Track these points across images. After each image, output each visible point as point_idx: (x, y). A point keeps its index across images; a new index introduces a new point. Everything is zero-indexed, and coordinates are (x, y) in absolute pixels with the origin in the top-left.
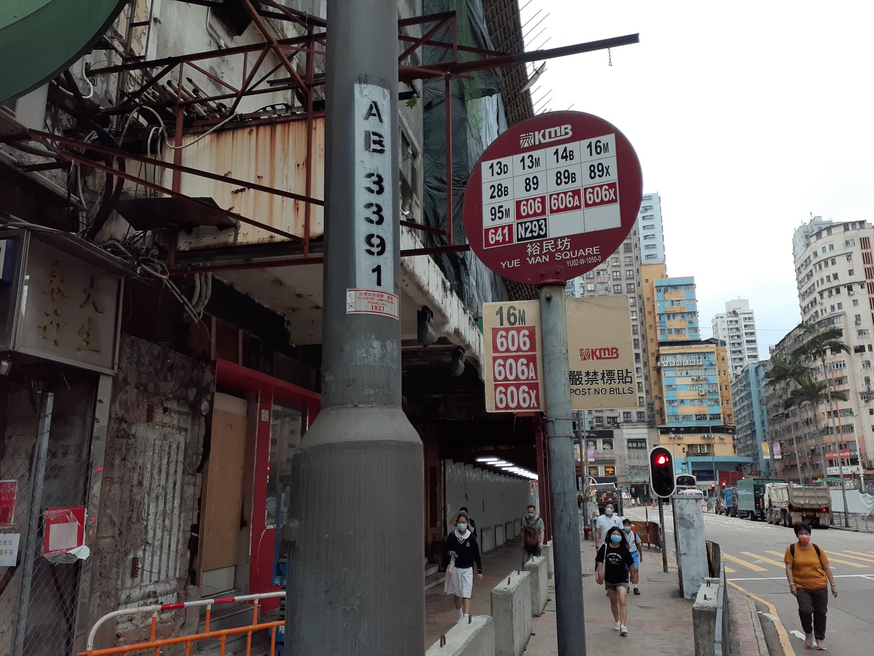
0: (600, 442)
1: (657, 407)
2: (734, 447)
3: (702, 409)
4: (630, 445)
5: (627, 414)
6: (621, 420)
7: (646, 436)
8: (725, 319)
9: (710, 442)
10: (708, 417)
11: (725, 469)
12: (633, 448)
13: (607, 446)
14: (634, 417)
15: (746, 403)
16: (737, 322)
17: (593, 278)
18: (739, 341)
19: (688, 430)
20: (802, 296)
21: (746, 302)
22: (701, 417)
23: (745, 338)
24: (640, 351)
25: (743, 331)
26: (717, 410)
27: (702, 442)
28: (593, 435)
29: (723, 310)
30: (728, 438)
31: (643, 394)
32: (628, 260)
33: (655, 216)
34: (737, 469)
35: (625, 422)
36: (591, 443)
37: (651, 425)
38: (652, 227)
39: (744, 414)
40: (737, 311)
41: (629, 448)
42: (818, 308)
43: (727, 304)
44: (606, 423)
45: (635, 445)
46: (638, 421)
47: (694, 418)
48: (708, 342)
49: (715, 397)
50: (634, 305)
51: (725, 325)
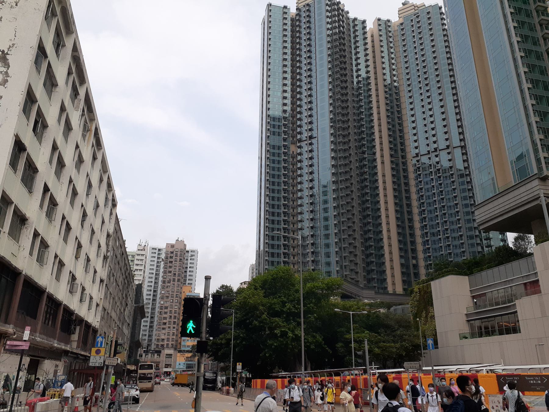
0: (156, 355)
1: (179, 341)
5: (168, 344)
6: (165, 346)
14: (170, 346)
19: (188, 351)
24: (176, 320)
31: (175, 337)
37: (175, 349)
44: (160, 347)
50: (177, 303)
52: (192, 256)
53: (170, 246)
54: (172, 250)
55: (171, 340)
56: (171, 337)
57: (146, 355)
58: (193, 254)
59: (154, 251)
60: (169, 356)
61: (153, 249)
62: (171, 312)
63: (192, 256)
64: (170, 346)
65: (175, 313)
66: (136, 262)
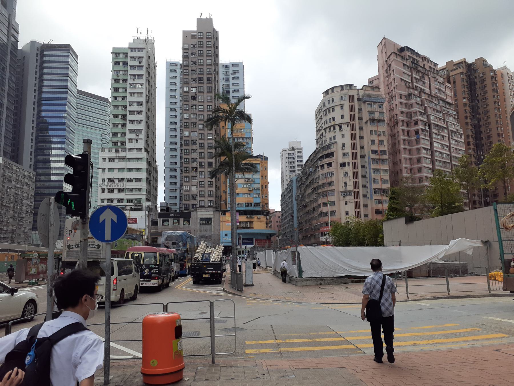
0: (182, 220)
2: (267, 224)
3: (249, 199)
4: (202, 222)
7: (212, 216)
8: (287, 152)
9: (252, 220)
10: (253, 205)
11: (259, 237)
12: (203, 224)
13: (186, 223)
15: (291, 200)
16: (293, 154)
17: (188, 110)
18: (294, 165)
20: (318, 131)
21: (299, 142)
22: (248, 205)
23: (297, 163)
25: (297, 159)
26: (258, 200)
27: (246, 220)
28: (177, 215)
29: (287, 147)
30: (263, 218)
31: (213, 189)
32: (209, 98)
33: (240, 78)
34: (267, 237)
35: (200, 207)
36: (176, 221)
38: (238, 84)
39: (289, 207)
40: (295, 148)
41: (200, 224)
42: (324, 139)
43: (290, 143)
45: (204, 222)
46: (209, 207)
47: (244, 205)
48: (256, 157)
49: (258, 192)
51: (287, 155)
52: (235, 72)
53: (189, 37)
54: (194, 41)
55: (207, 195)
56: (207, 189)
57: (163, 222)
58: (235, 69)
59: (174, 68)
60: (207, 221)
61: (172, 64)
62: (202, 148)
63: (235, 72)
64: (206, 206)
65: (210, 148)
66: (131, 62)
